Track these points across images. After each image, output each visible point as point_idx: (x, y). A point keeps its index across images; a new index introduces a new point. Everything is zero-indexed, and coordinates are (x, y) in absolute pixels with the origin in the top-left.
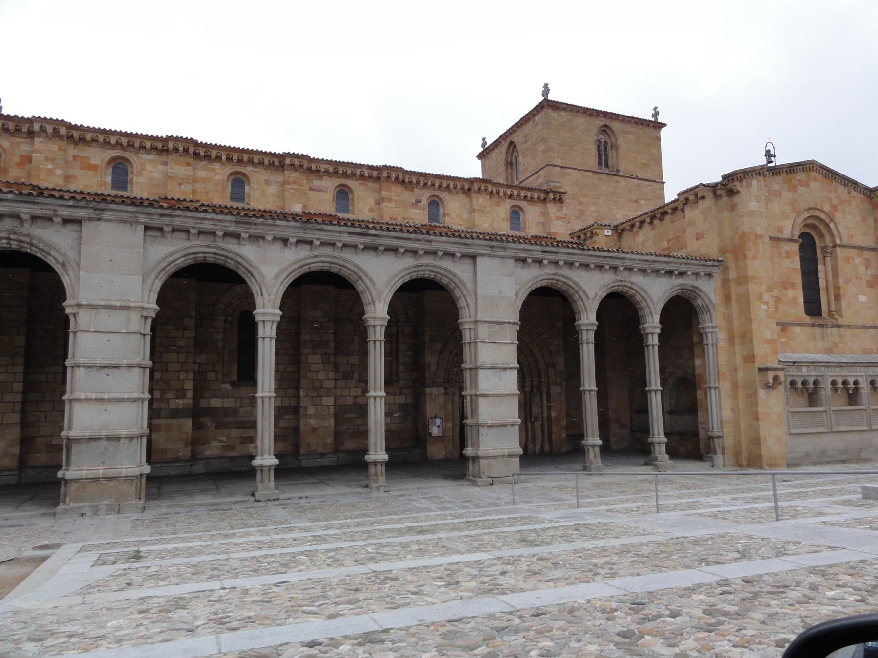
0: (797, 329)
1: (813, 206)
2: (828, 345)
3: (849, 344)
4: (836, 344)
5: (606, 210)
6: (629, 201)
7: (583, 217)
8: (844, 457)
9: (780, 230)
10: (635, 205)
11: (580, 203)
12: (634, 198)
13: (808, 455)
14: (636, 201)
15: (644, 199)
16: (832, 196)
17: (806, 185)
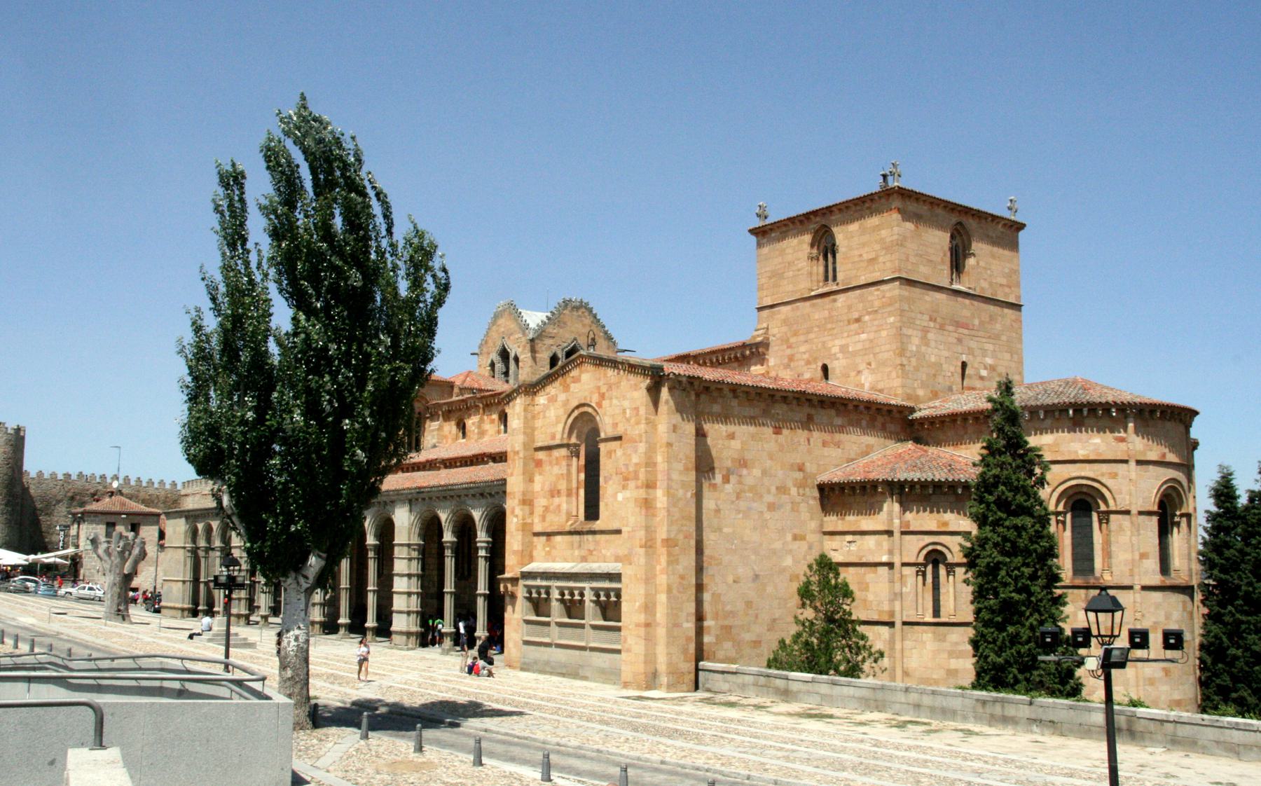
0: (558, 538)
1: (583, 402)
2: (583, 553)
3: (603, 551)
4: (591, 552)
5: (820, 345)
6: (849, 322)
7: (792, 364)
8: (564, 671)
9: (553, 437)
10: (856, 325)
11: (790, 347)
12: (856, 315)
13: (536, 662)
14: (858, 320)
15: (869, 313)
16: (601, 383)
17: (577, 380)
